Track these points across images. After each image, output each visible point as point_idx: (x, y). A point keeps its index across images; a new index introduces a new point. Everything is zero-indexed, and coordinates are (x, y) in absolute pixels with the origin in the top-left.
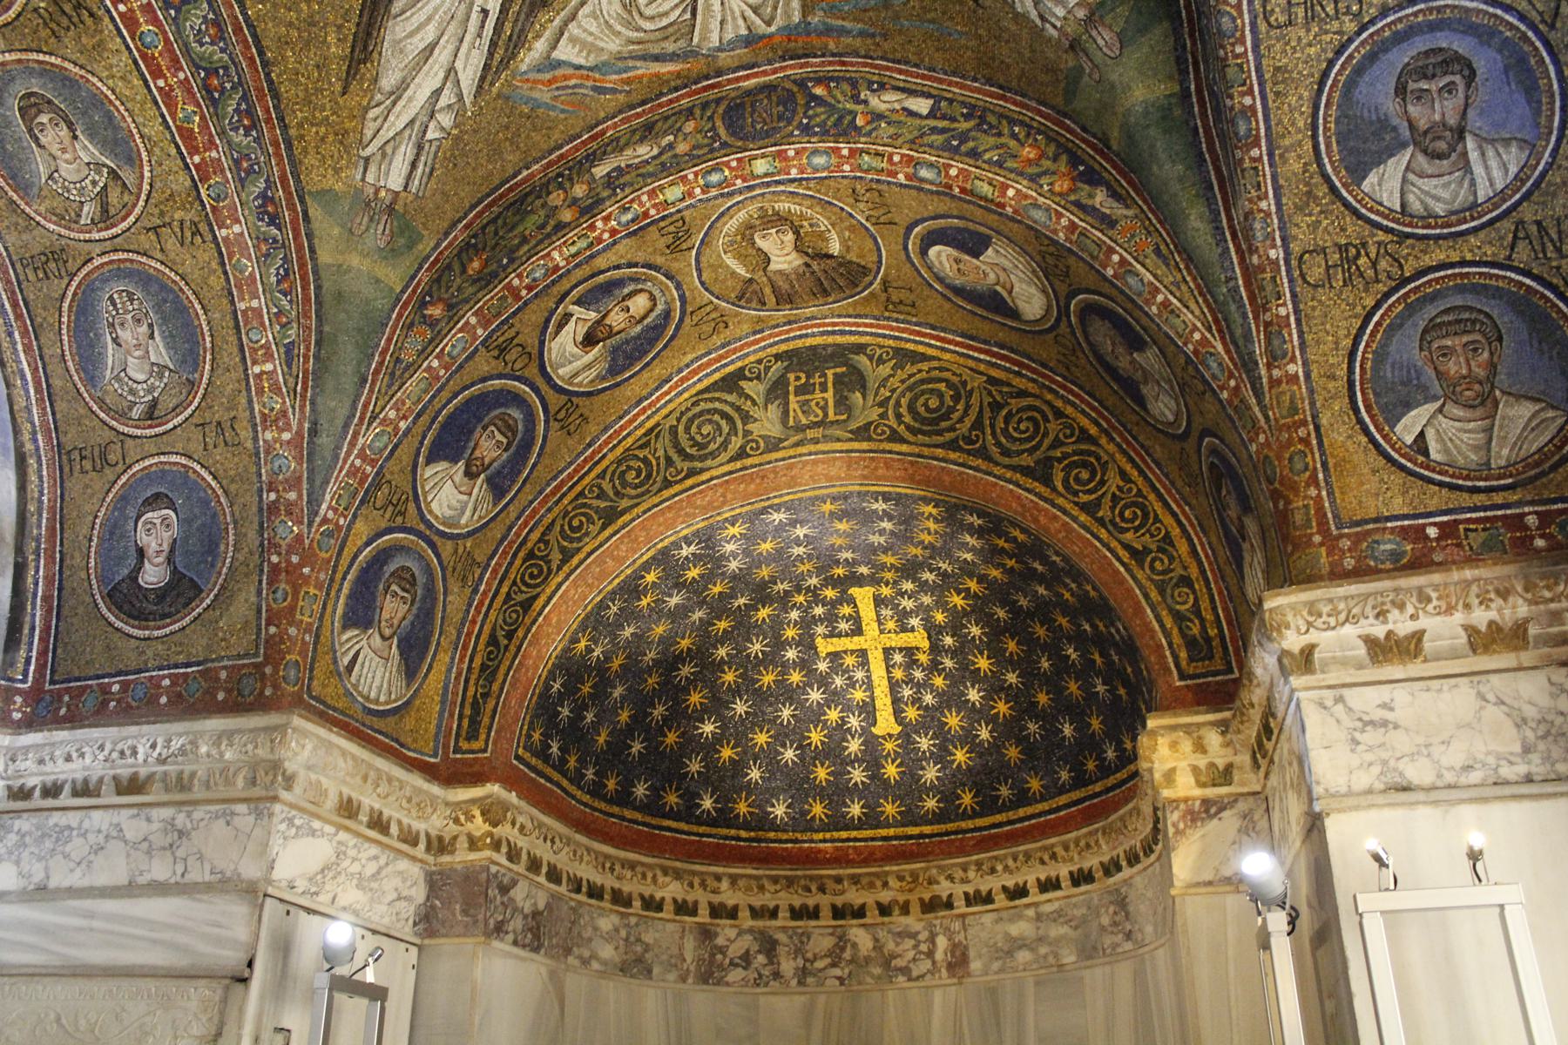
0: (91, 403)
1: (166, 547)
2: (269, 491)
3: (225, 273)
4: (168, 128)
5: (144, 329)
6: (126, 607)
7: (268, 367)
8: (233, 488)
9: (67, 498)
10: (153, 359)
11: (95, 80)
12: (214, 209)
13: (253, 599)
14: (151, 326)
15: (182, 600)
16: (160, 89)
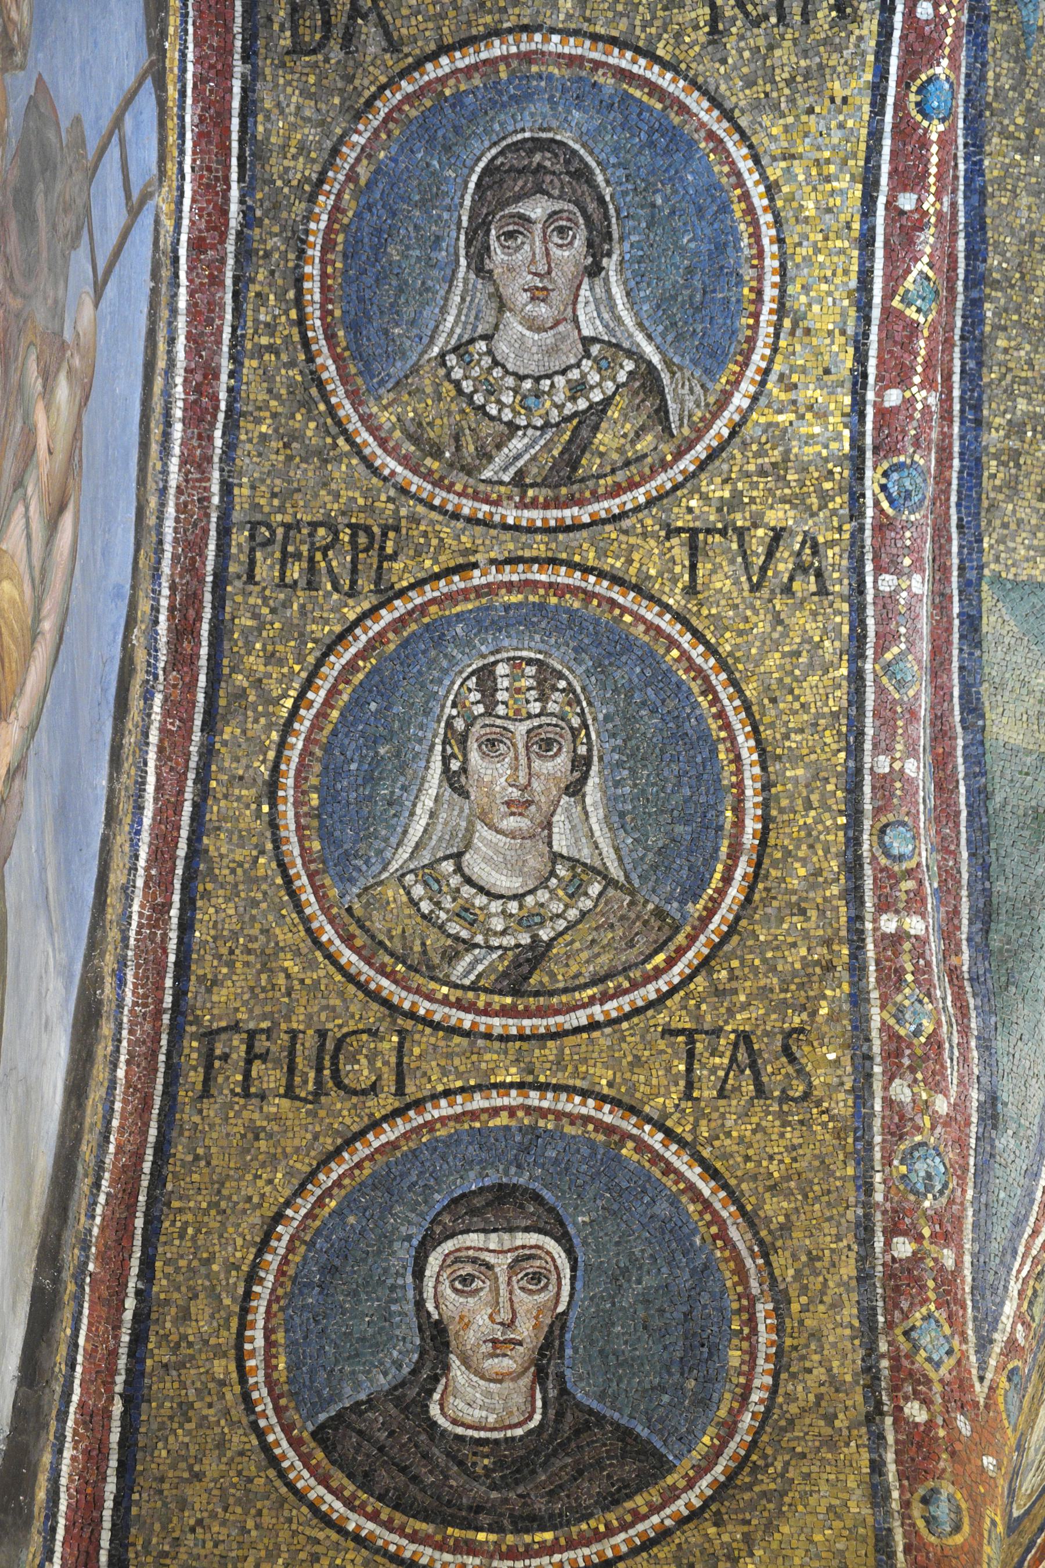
0: (320, 921)
1: (525, 1330)
2: (890, 1233)
3: (857, 677)
4: (864, 308)
5: (559, 765)
6: (384, 1478)
7: (915, 925)
8: (775, 1208)
9: (180, 1151)
10: (560, 845)
11: (739, 153)
12: (881, 527)
13: (858, 1507)
14: (581, 765)
15: (590, 1489)
16: (894, 211)
